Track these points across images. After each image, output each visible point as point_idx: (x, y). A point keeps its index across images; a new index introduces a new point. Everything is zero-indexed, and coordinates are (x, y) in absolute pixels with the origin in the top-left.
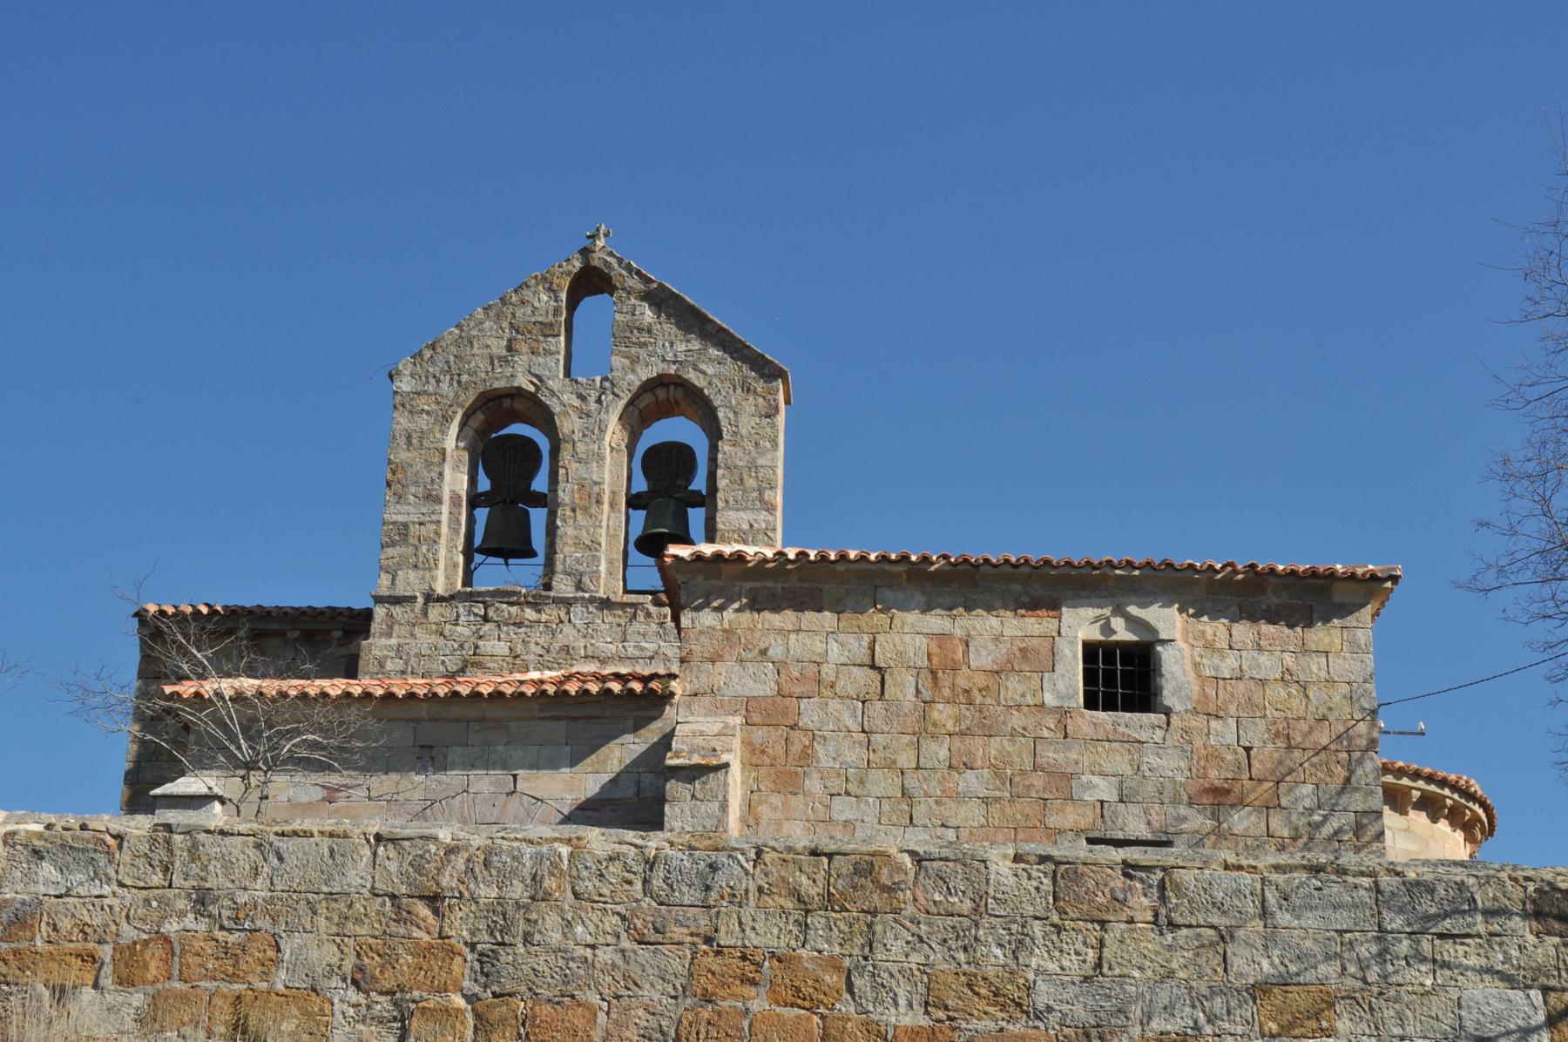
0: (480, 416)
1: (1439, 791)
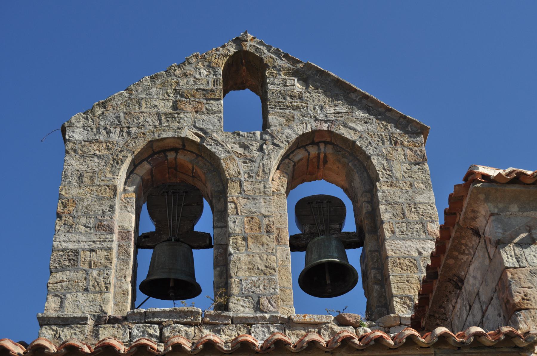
0: (146, 166)
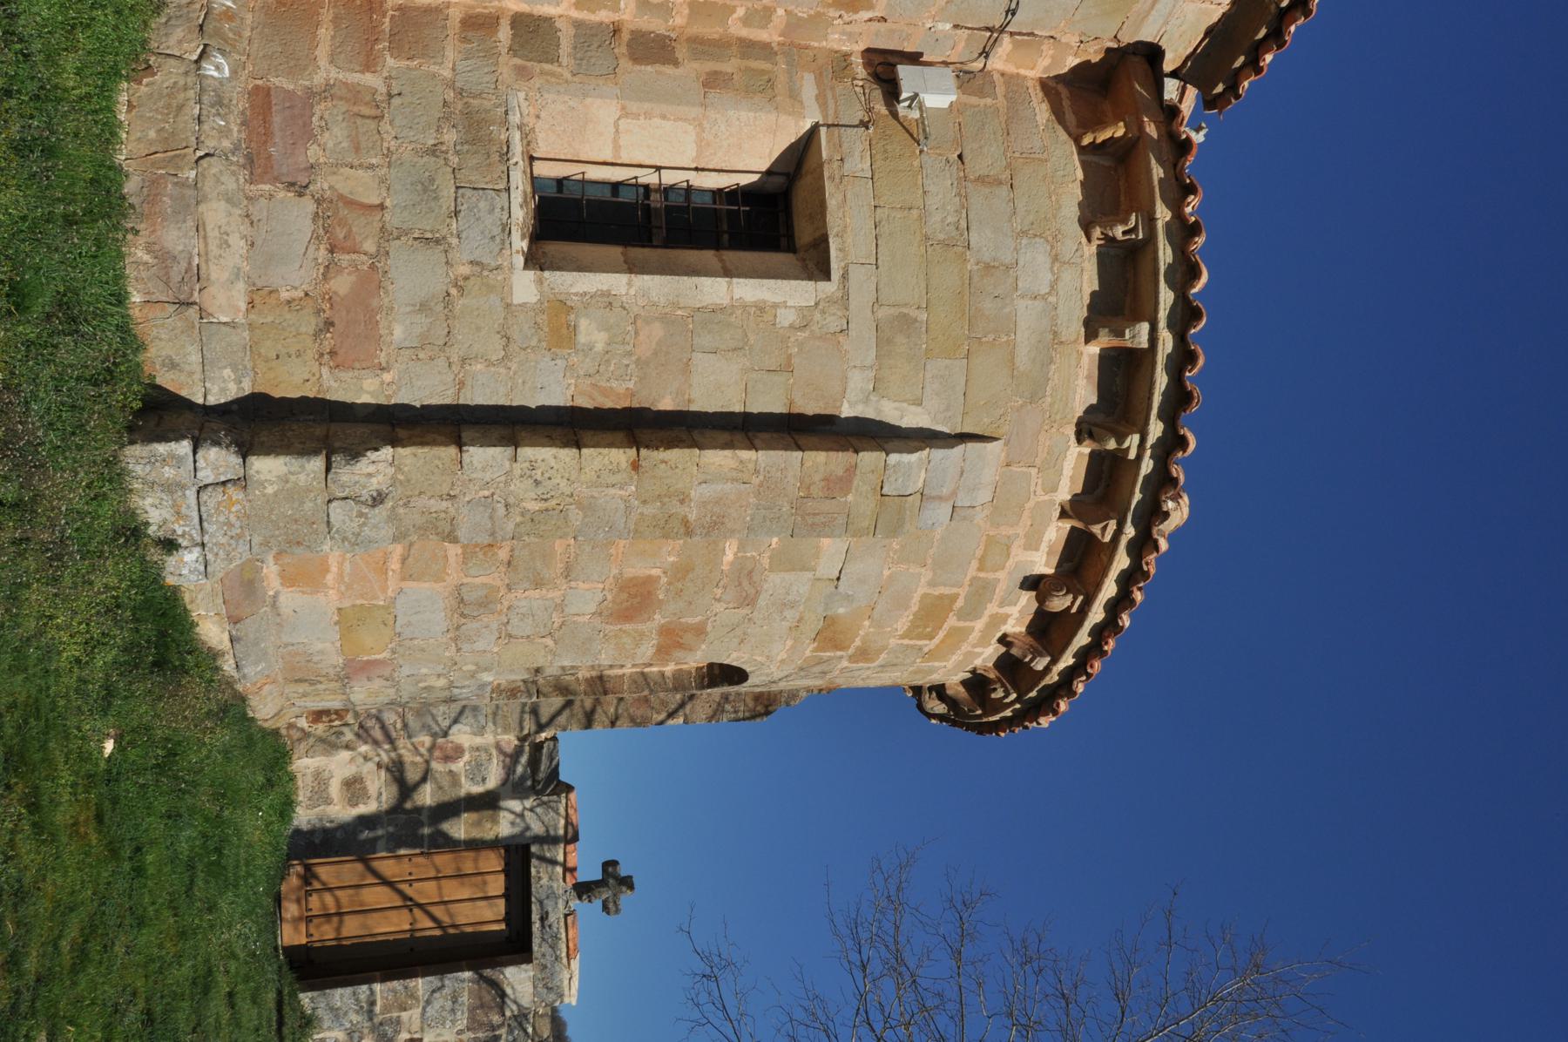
1: (1157, 399)
